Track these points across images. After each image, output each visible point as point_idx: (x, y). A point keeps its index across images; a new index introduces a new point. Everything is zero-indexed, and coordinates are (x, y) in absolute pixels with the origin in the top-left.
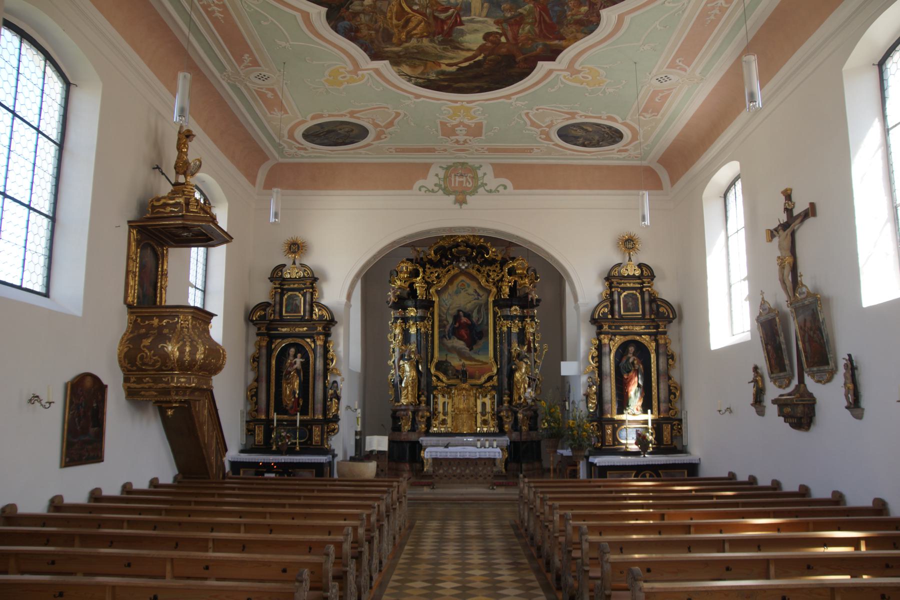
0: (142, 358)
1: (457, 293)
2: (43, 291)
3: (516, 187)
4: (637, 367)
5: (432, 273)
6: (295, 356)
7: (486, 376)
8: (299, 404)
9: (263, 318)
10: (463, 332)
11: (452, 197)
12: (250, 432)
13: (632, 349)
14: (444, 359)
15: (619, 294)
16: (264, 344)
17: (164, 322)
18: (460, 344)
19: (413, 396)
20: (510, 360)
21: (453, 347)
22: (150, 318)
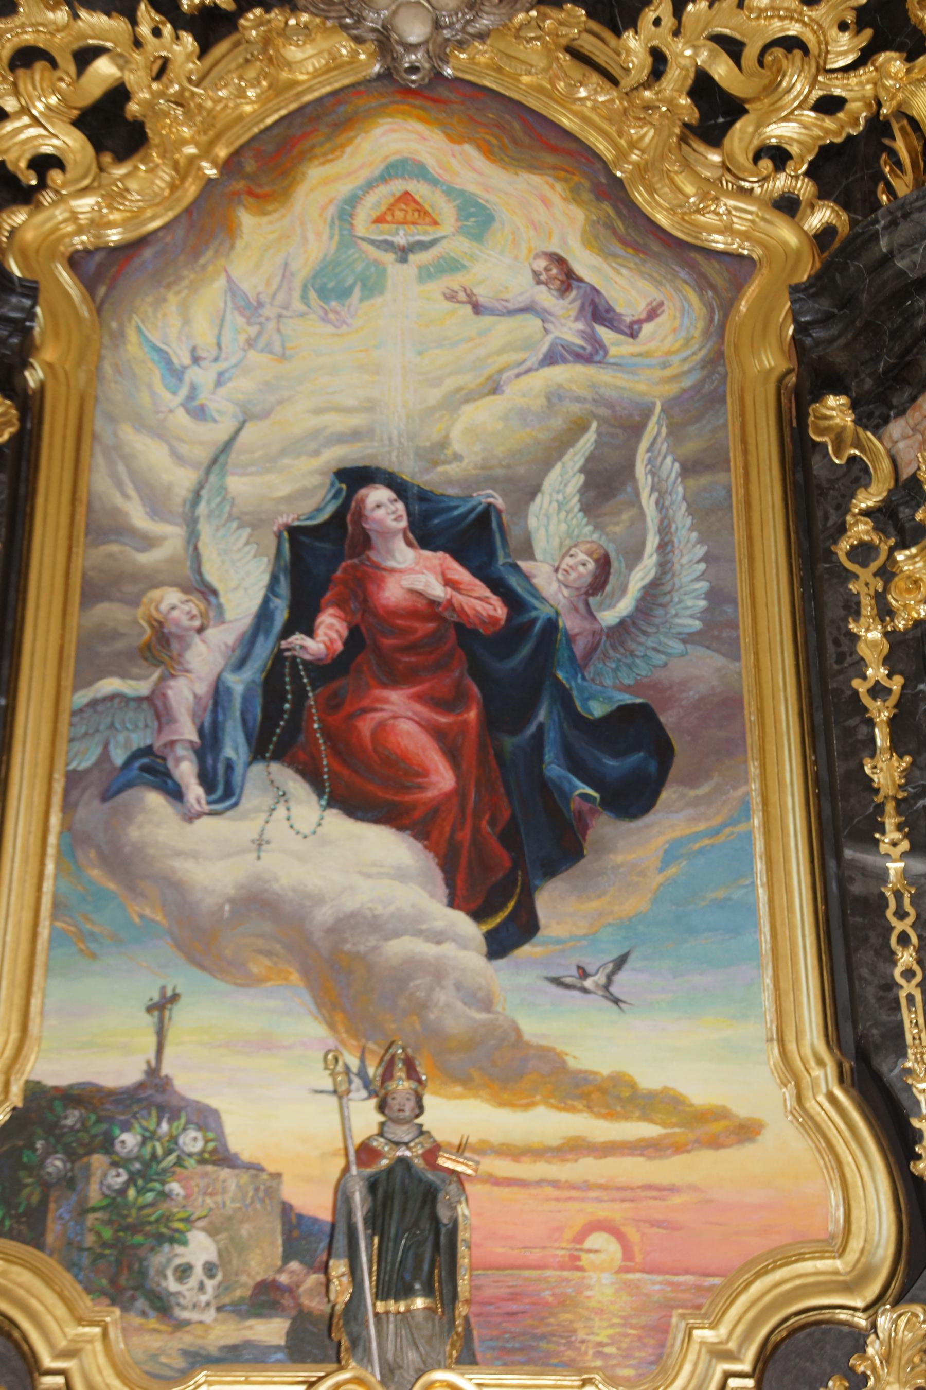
1: (332, 287)
10: (401, 718)
14: (119, 1071)
18: (371, 873)
21: (257, 902)
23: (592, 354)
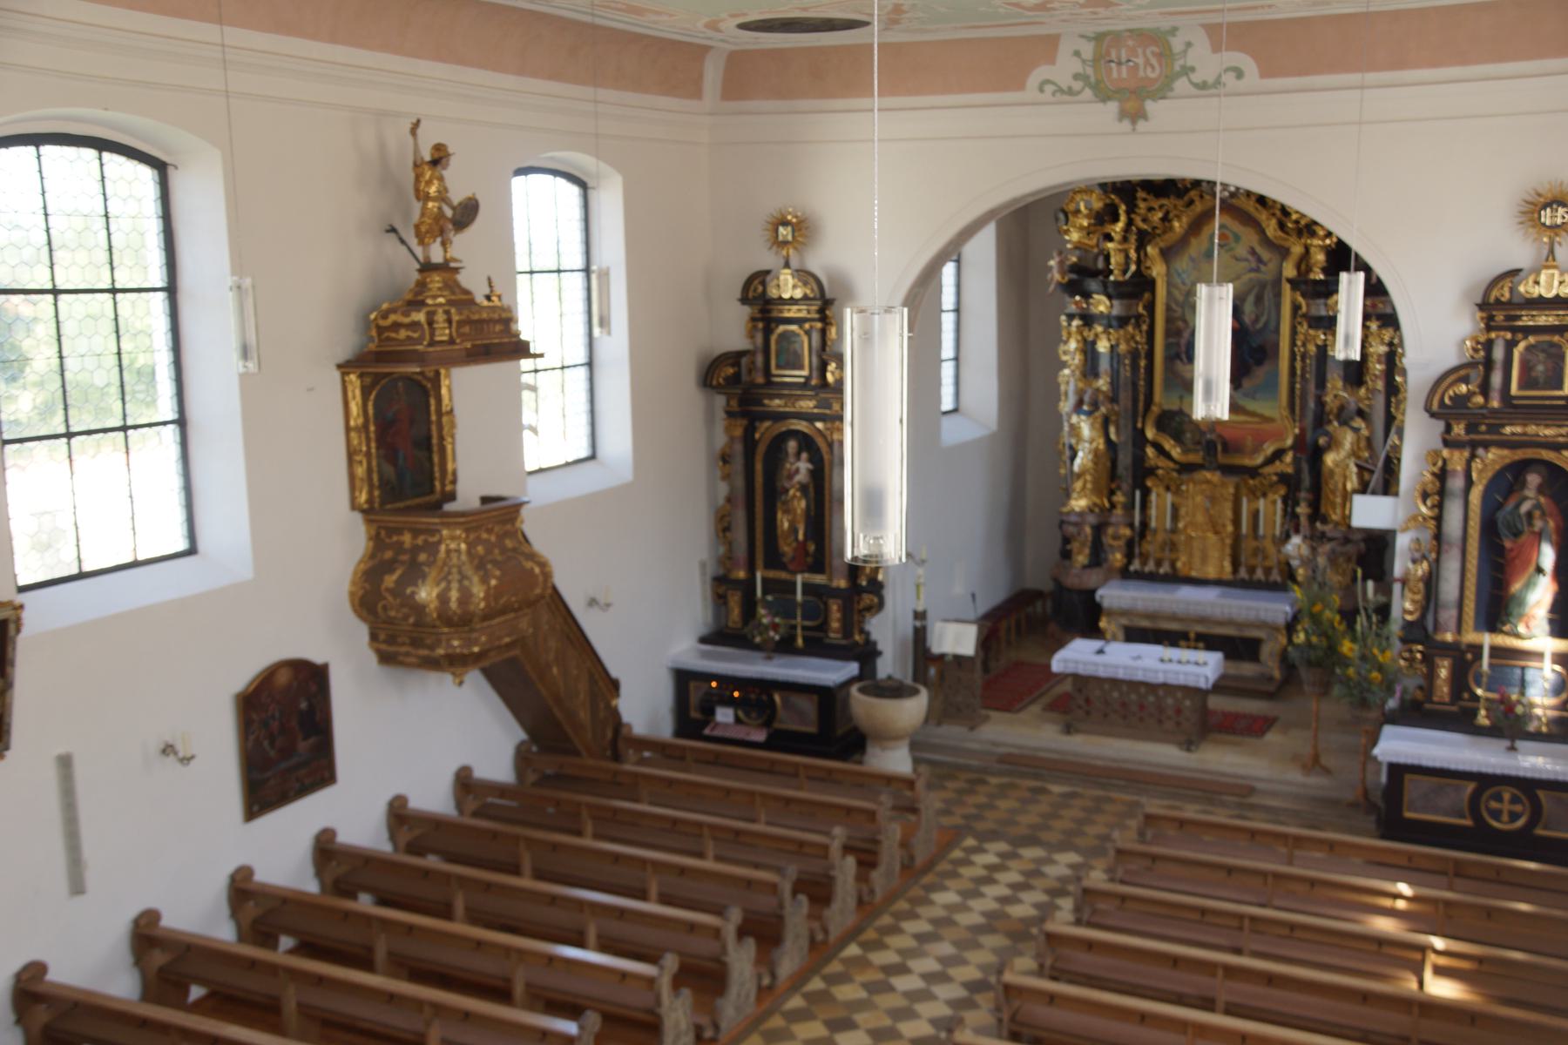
0: (385, 608)
2: (182, 545)
3: (1268, 70)
4: (1538, 524)
5: (1150, 209)
6: (798, 456)
7: (1269, 449)
8: (807, 554)
9: (735, 380)
11: (1113, 107)
12: (720, 599)
13: (1533, 479)
14: (1175, 407)
15: (1510, 346)
16: (738, 432)
17: (420, 541)
19: (1097, 490)
20: (1321, 419)
22: (399, 531)
23: (1257, 270)
